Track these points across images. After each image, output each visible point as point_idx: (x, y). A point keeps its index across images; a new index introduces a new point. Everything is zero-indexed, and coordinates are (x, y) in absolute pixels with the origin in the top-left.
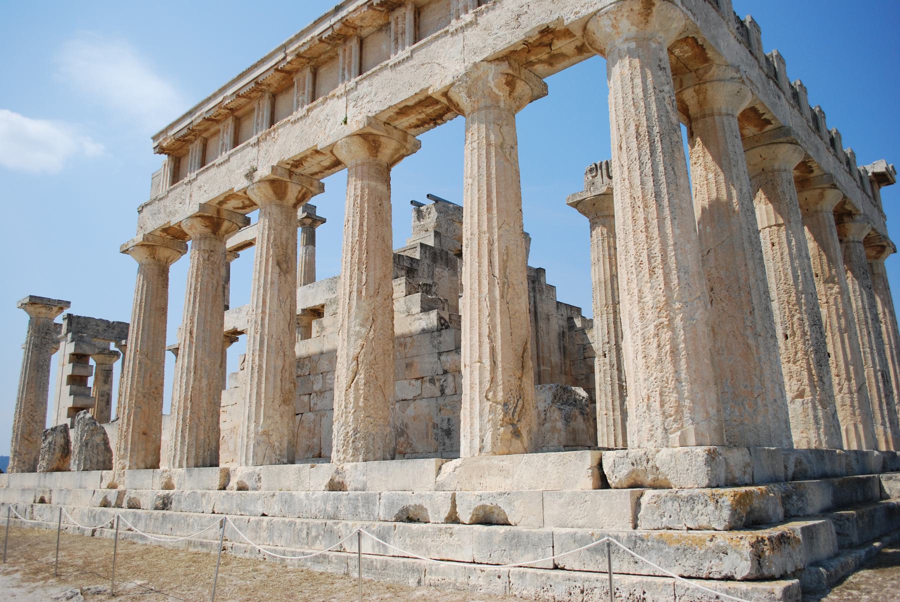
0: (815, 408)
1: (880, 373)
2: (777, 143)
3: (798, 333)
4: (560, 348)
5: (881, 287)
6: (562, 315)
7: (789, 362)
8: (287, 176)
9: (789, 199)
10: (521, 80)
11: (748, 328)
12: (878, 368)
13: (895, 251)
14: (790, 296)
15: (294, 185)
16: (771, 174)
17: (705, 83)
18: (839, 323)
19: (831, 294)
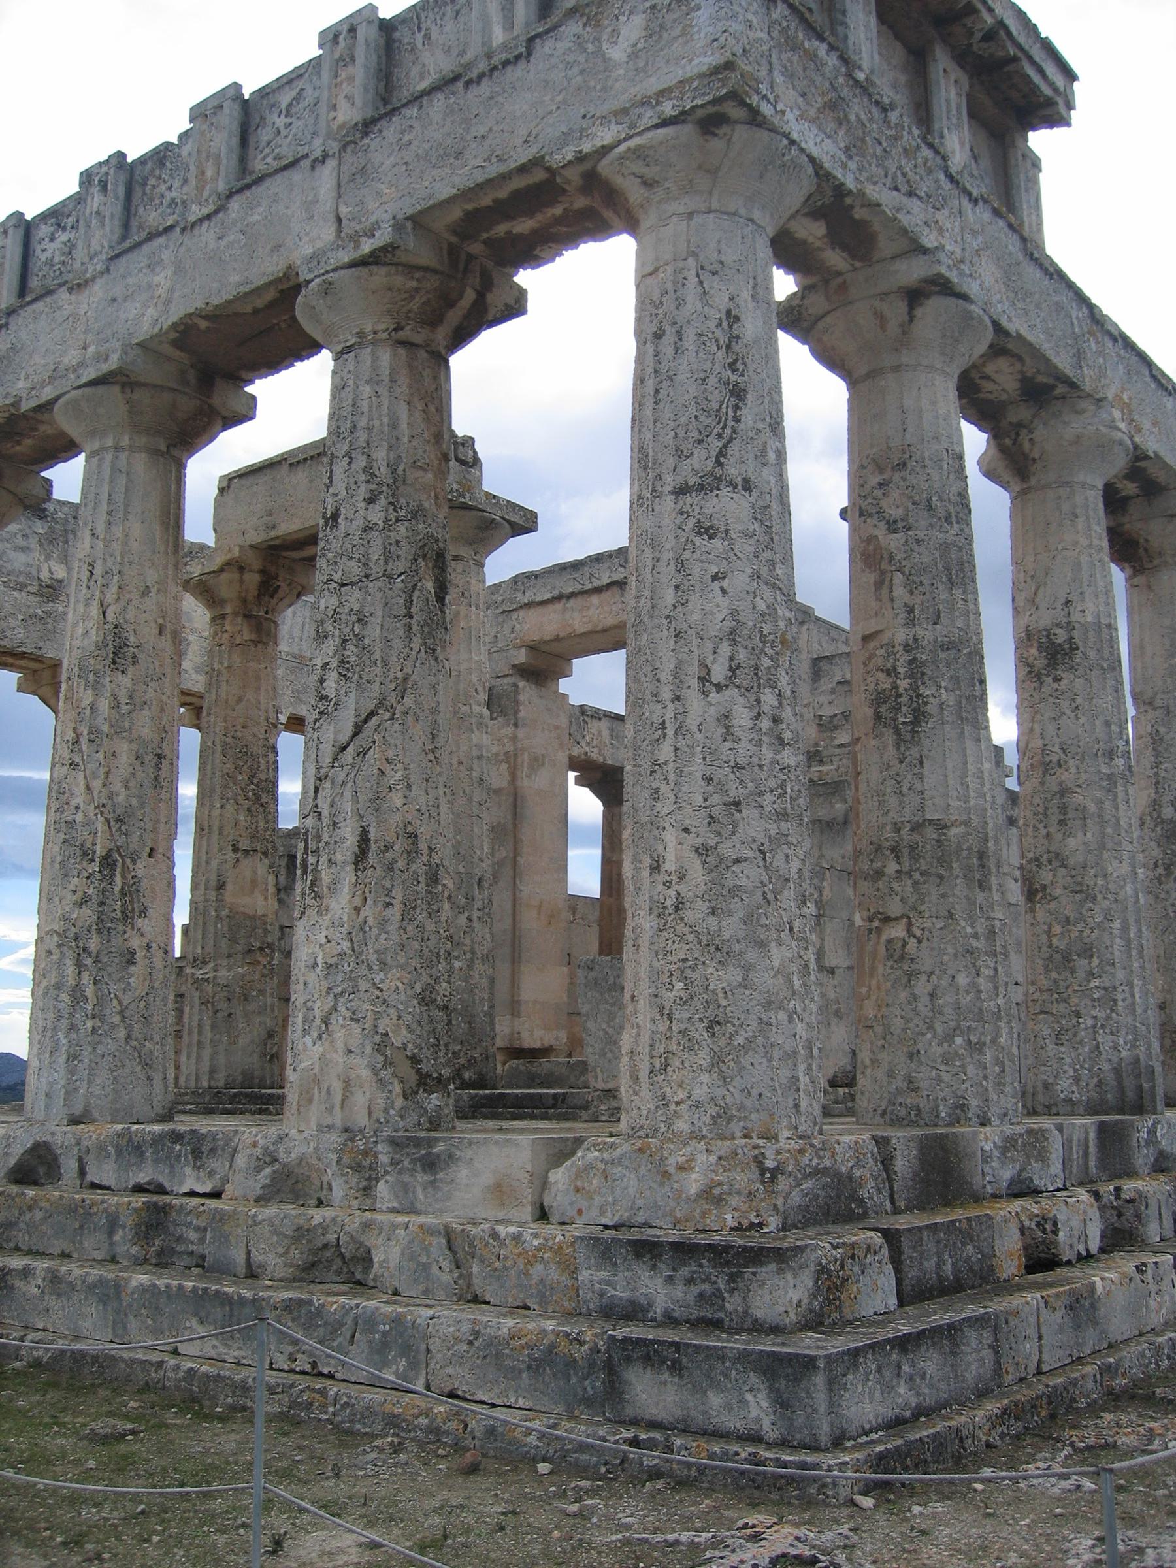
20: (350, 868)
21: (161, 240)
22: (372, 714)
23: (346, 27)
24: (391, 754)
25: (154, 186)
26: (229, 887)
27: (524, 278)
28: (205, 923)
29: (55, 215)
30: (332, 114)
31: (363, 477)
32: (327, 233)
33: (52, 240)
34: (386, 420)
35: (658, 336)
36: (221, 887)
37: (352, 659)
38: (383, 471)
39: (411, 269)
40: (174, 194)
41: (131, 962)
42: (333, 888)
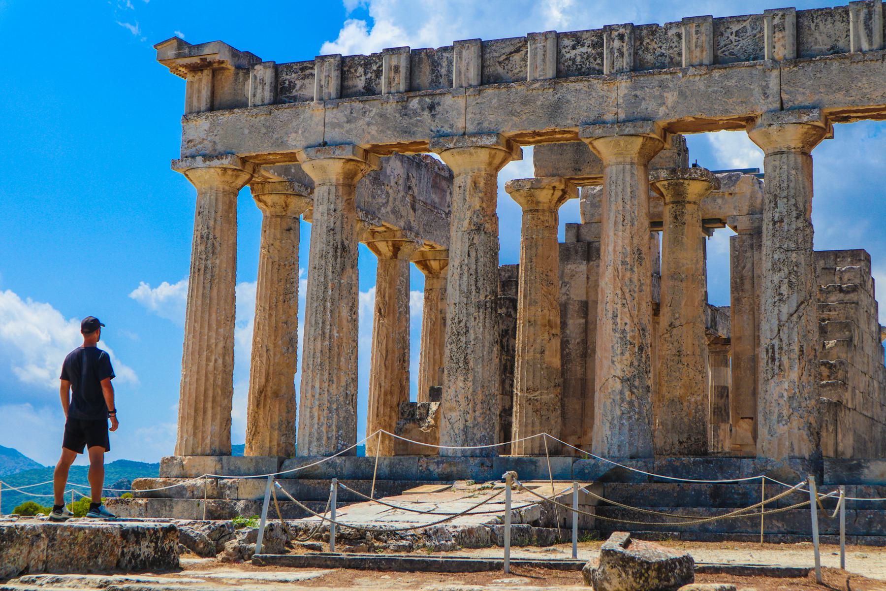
8: (371, 237)
10: (264, 194)
15: (379, 243)
20: (797, 361)
21: (669, 76)
22: (802, 303)
23: (781, 13)
24: (808, 318)
25: (648, 43)
26: (547, 353)
27: (835, 125)
28: (534, 371)
29: (577, 37)
30: (773, 50)
31: (793, 208)
32: (777, 105)
33: (574, 48)
34: (801, 186)
36: (542, 352)
37: (794, 281)
38: (801, 207)
39: (815, 127)
40: (663, 51)
41: (649, 391)
42: (791, 367)
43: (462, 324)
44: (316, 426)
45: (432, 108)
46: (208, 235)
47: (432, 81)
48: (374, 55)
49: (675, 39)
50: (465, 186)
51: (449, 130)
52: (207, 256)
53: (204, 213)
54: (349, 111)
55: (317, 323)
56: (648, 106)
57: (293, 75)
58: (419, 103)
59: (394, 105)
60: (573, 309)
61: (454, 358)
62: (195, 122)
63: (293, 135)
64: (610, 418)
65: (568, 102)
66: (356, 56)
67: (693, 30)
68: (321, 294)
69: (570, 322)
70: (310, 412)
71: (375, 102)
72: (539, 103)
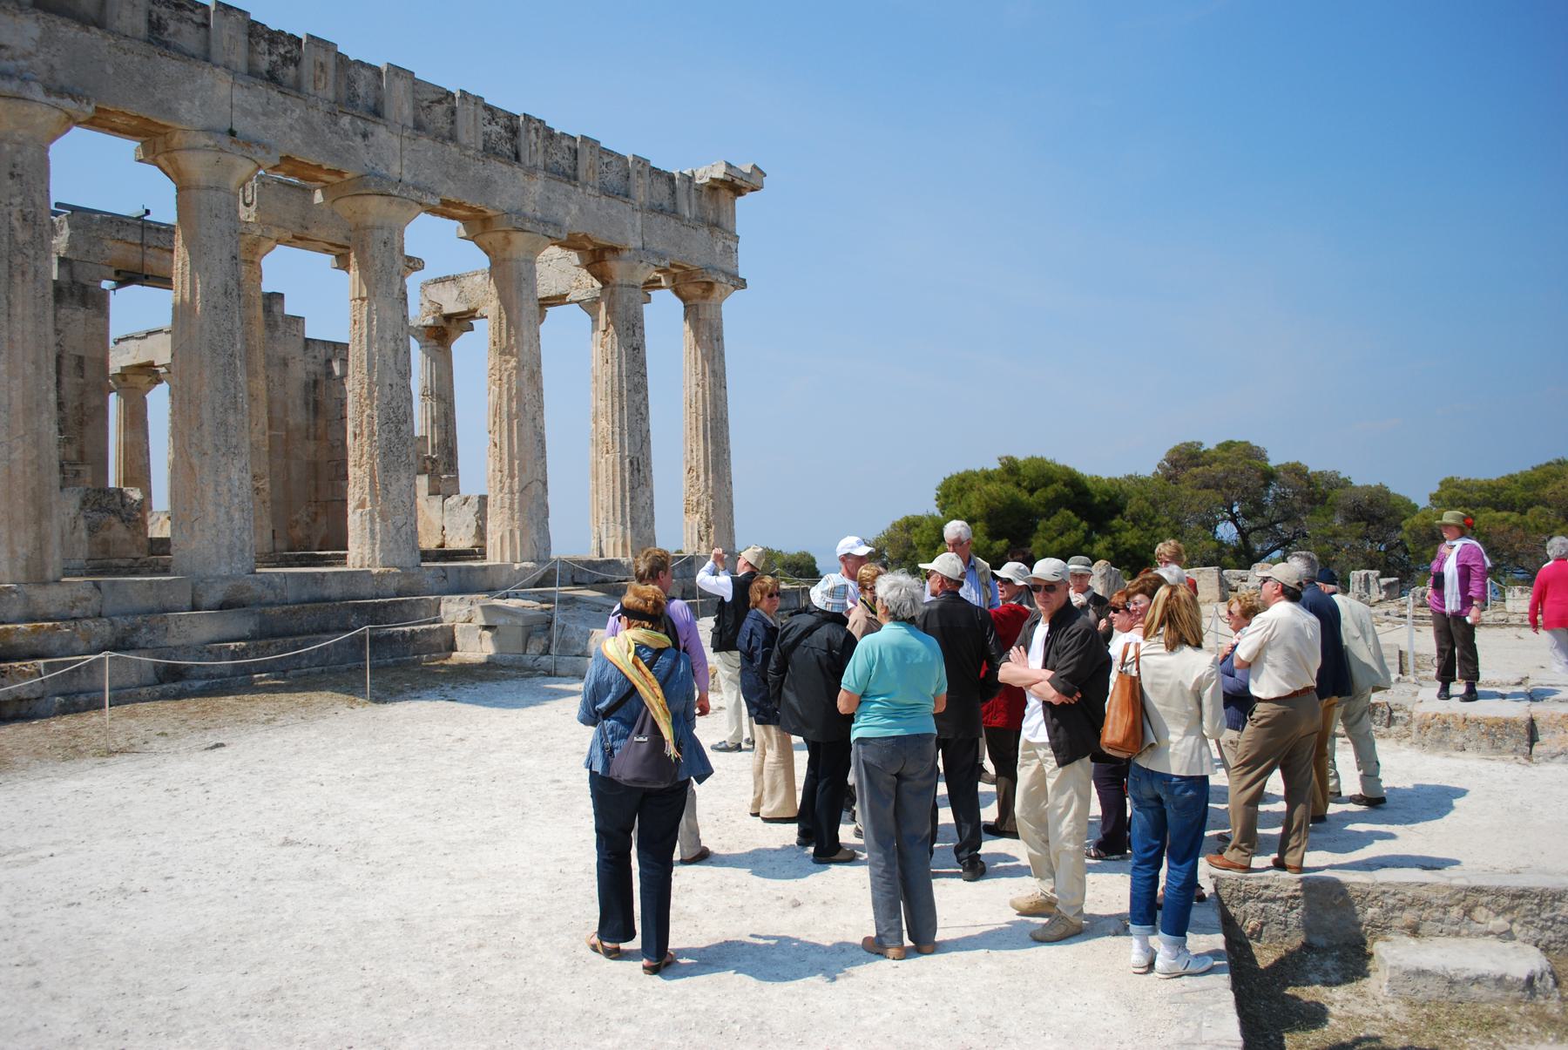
0: (372, 521)
1: (628, 460)
2: (362, 195)
3: (366, 432)
4: (307, 404)
5: (704, 338)
6: (315, 357)
7: (355, 465)
9: (379, 266)
11: (193, 446)
12: (627, 453)
13: (742, 284)
14: (363, 388)
16: (363, 232)
17: (172, 151)
18: (509, 407)
19: (506, 370)
21: (571, 188)
35: (718, 340)
43: (401, 410)
44: (237, 533)
45: (365, 136)
46: (34, 217)
47: (349, 99)
48: (281, 33)
49: (567, 151)
50: (393, 244)
51: (385, 172)
52: (36, 253)
53: (24, 178)
54: (265, 101)
55: (226, 387)
56: (558, 212)
57: (163, 9)
58: (351, 123)
59: (321, 114)
60: (69, 363)
61: (394, 450)
62: (11, 18)
63: (185, 104)
64: (535, 521)
65: (495, 182)
66: (257, 23)
67: (587, 150)
68: (227, 346)
69: (65, 380)
70: (228, 513)
71: (298, 101)
72: (471, 173)
